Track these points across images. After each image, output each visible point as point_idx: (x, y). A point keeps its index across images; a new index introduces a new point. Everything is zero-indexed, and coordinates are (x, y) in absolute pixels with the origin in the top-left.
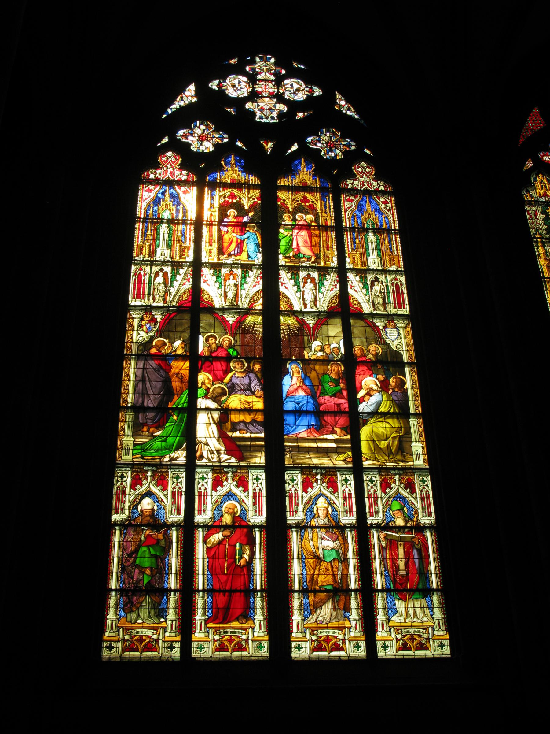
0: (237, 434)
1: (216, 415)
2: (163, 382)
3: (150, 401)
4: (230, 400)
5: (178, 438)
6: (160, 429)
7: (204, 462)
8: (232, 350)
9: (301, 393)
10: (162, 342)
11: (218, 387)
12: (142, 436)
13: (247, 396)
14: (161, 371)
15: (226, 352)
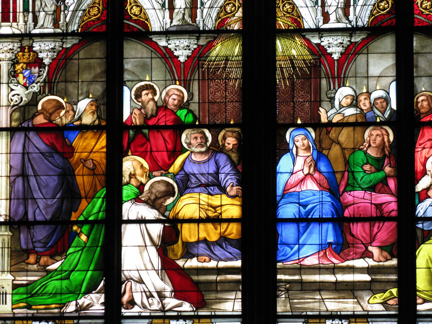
0: (193, 263)
1: (156, 230)
2: (59, 175)
3: (37, 211)
4: (180, 205)
5: (89, 273)
6: (57, 258)
7: (136, 310)
8: (185, 111)
9: (311, 186)
10: (54, 103)
11: (159, 182)
12: (27, 271)
13: (212, 195)
14: (56, 156)
15: (173, 117)
